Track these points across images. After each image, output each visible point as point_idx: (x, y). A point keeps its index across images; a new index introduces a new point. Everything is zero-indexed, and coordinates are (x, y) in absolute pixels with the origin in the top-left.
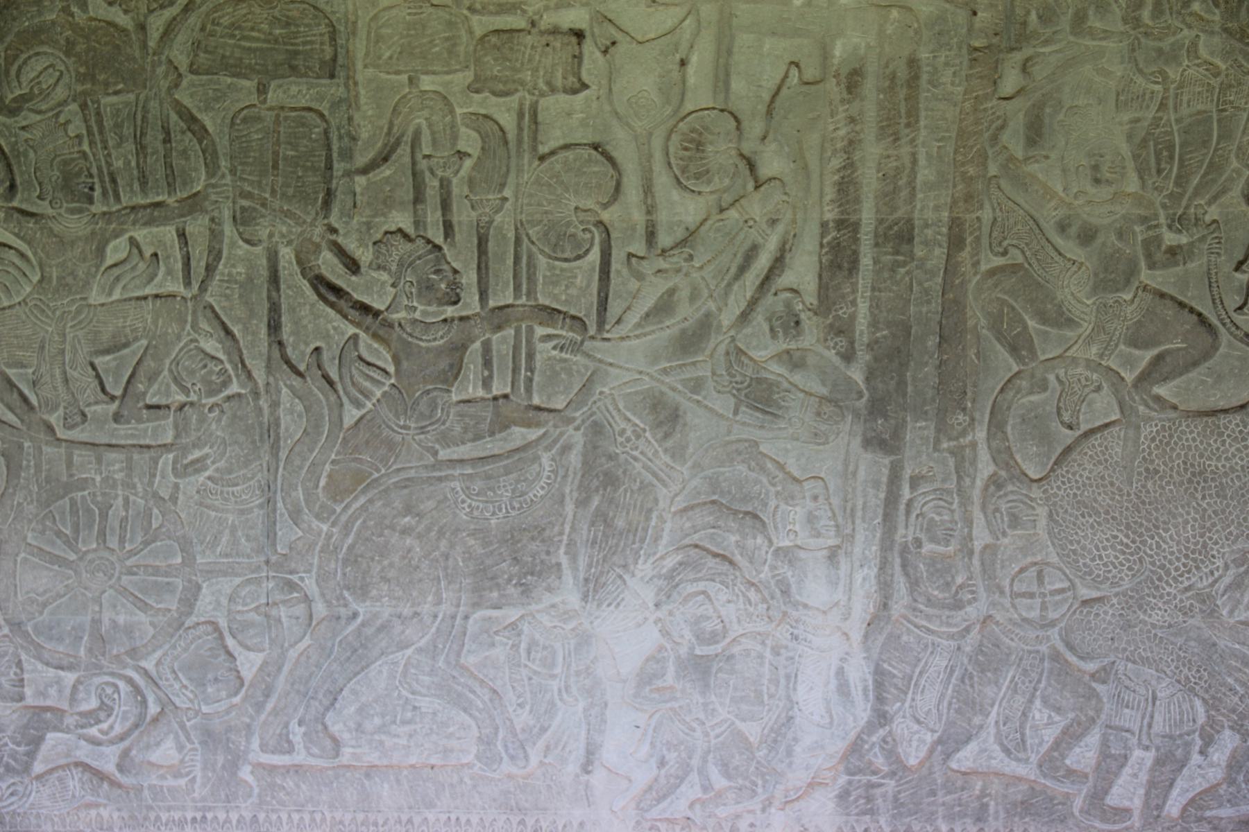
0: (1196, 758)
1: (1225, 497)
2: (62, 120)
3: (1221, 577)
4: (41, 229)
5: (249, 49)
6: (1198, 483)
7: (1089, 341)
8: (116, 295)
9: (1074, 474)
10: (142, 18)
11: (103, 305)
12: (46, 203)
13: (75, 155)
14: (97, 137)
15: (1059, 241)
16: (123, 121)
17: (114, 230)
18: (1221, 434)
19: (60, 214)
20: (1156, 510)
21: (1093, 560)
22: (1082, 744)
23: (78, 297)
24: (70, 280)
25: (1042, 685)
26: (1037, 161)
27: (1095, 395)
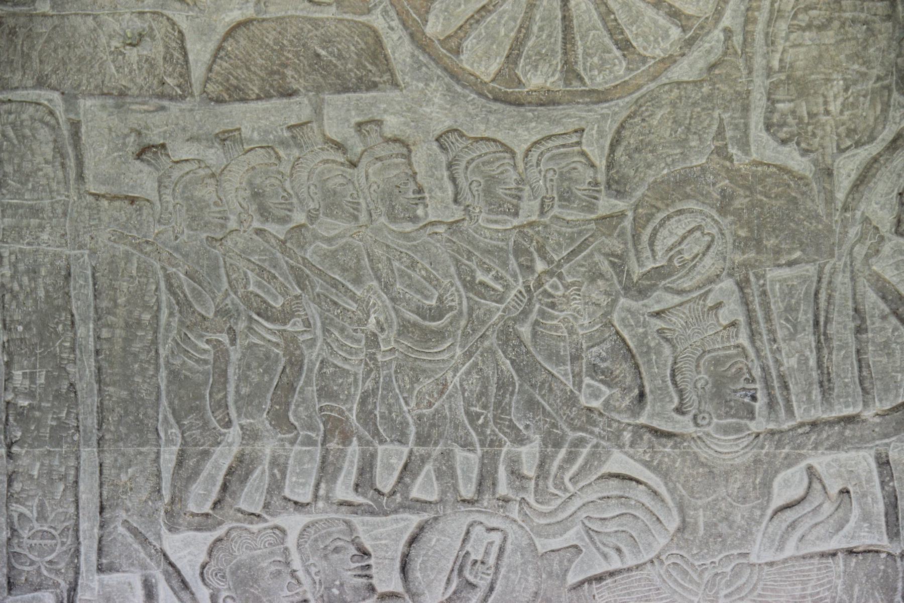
2: (710, 302)
4: (683, 455)
8: (790, 550)
10: (829, 161)
11: (771, 564)
12: (688, 418)
13: (733, 351)
14: (763, 327)
16: (798, 303)
17: (787, 456)
19: (708, 435)
23: (735, 552)
24: (723, 528)
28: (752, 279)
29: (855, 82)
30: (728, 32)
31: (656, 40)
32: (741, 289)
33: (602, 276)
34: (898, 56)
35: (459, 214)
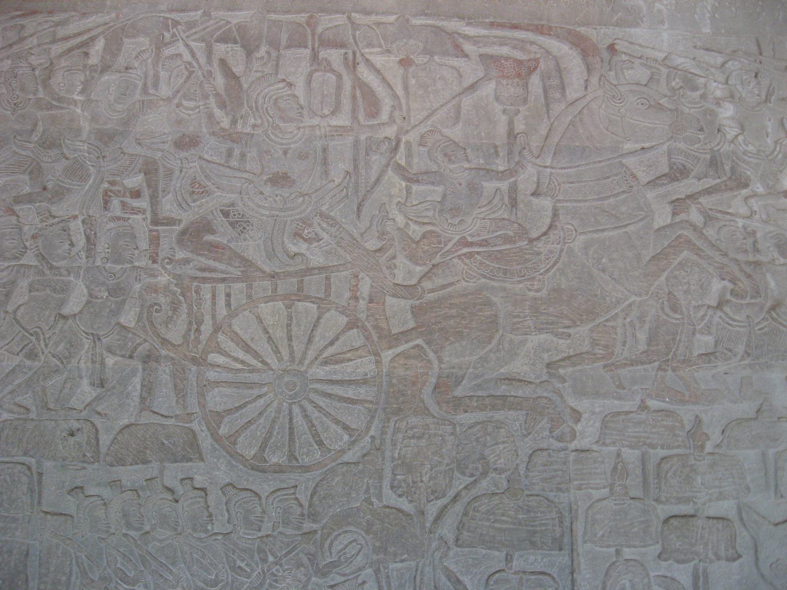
2: (360, 581)
5: (500, 529)
28: (382, 569)
29: (436, 466)
30: (373, 437)
31: (336, 441)
32: (376, 574)
33: (302, 565)
34: (457, 454)
35: (230, 528)
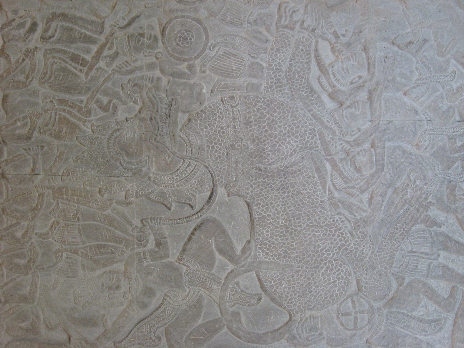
0: (443, 229)
1: (300, 215)
3: (345, 217)
6: (292, 229)
7: (210, 290)
9: (287, 297)
15: (152, 307)
18: (264, 217)
20: (307, 252)
21: (336, 286)
22: (436, 289)
25: (406, 312)
26: (106, 321)
27: (241, 286)
